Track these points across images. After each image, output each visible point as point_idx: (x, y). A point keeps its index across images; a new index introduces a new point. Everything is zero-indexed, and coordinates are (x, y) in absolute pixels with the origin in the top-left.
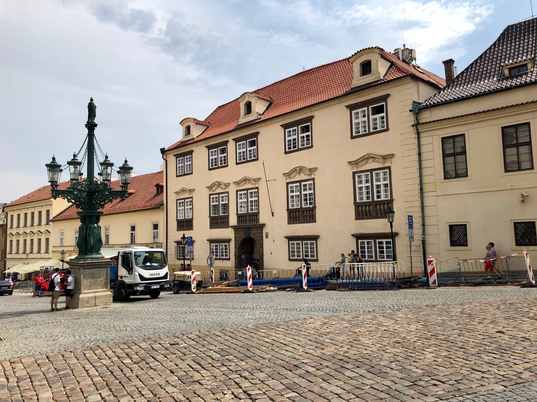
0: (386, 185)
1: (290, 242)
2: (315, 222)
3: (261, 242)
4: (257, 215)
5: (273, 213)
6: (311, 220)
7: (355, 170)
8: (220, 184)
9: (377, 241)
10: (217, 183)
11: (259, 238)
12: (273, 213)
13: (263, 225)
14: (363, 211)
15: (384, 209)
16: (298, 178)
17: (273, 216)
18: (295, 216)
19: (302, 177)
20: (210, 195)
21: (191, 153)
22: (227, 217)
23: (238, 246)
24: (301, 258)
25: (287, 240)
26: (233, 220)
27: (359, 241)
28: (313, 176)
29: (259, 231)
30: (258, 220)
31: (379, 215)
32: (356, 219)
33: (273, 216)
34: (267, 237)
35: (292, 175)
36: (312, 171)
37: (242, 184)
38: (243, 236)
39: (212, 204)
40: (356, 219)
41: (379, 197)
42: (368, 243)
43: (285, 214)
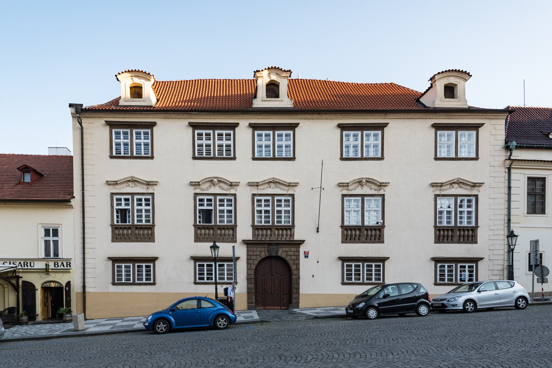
0: (469, 213)
1: (345, 264)
2: (383, 242)
3: (296, 262)
4: (291, 228)
5: (318, 228)
6: (377, 240)
7: (438, 192)
8: (219, 181)
9: (459, 265)
10: (216, 180)
11: (294, 258)
12: (318, 228)
13: (302, 242)
14: (443, 235)
15: (468, 235)
16: (359, 191)
17: (318, 232)
18: (351, 234)
19: (366, 190)
20: (196, 194)
21: (151, 125)
22: (233, 228)
23: (254, 267)
24: (361, 281)
25: (340, 262)
26: (244, 232)
27: (439, 265)
28: (382, 192)
29: (293, 249)
30: (292, 235)
31: (462, 240)
32: (436, 242)
33: (318, 232)
34: (306, 257)
35: (350, 188)
36: (382, 185)
37: (262, 187)
38: (263, 255)
39: (198, 208)
40: (436, 242)
41: (461, 222)
42: (449, 267)
43: (339, 232)
